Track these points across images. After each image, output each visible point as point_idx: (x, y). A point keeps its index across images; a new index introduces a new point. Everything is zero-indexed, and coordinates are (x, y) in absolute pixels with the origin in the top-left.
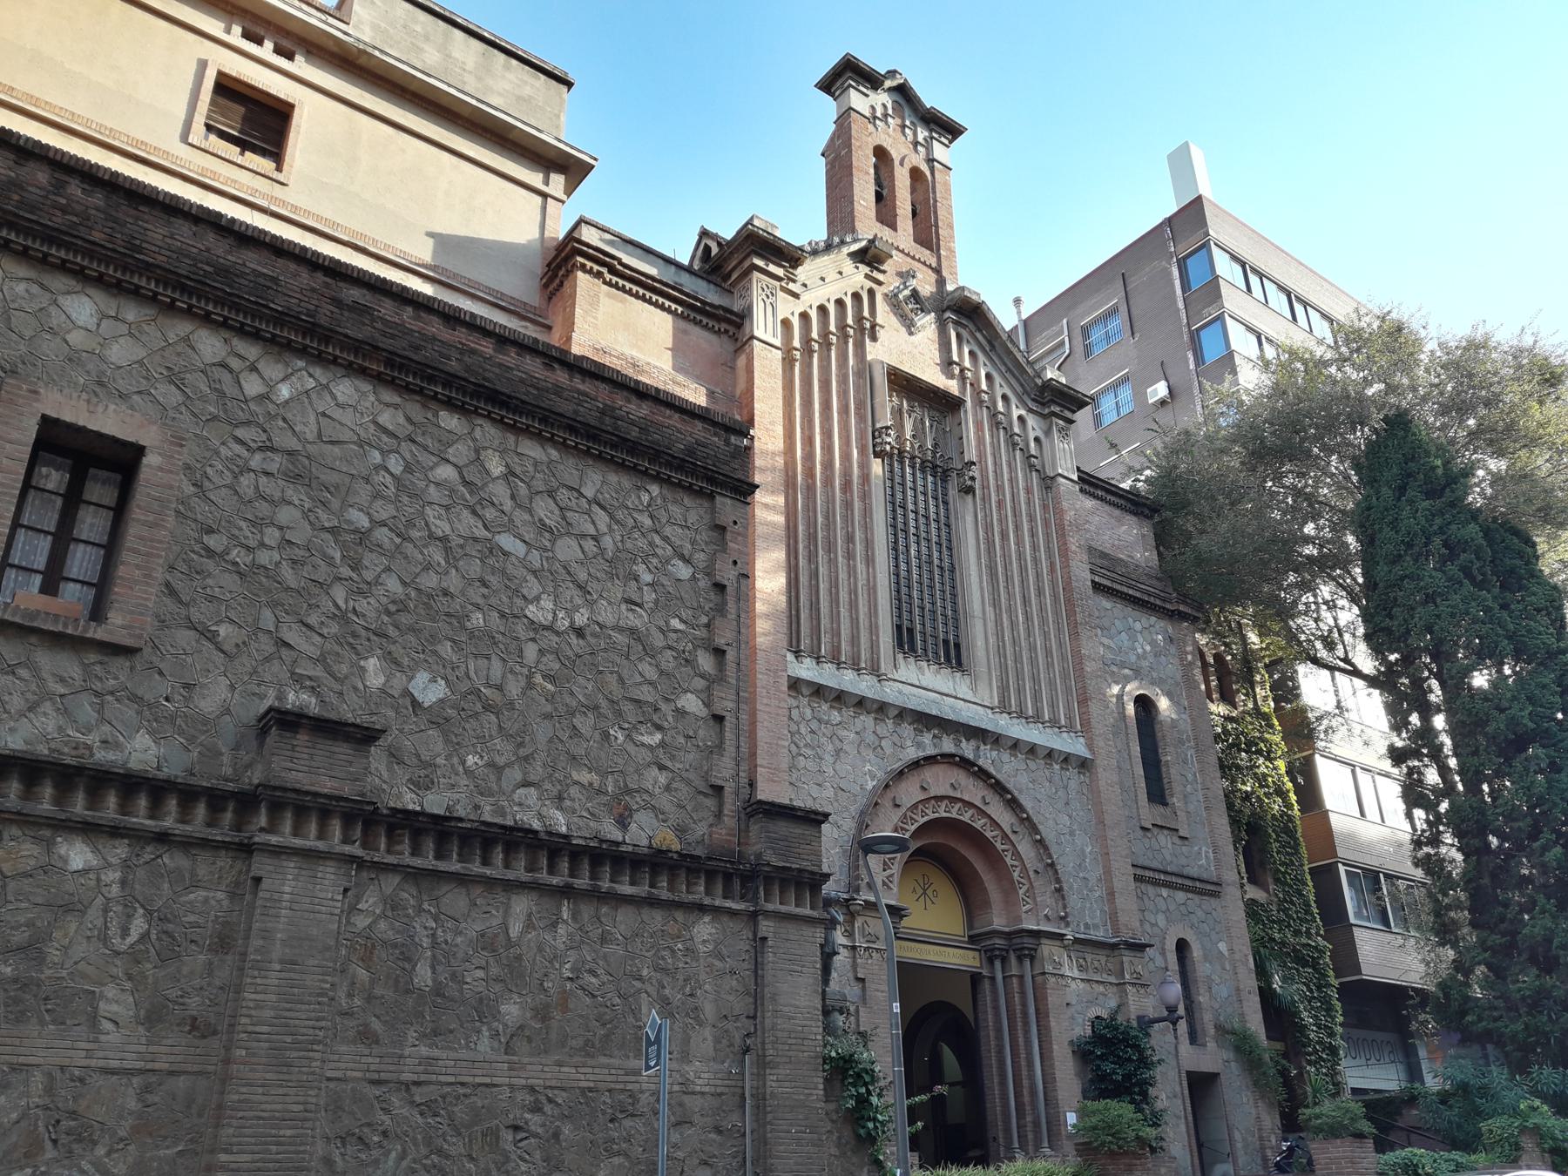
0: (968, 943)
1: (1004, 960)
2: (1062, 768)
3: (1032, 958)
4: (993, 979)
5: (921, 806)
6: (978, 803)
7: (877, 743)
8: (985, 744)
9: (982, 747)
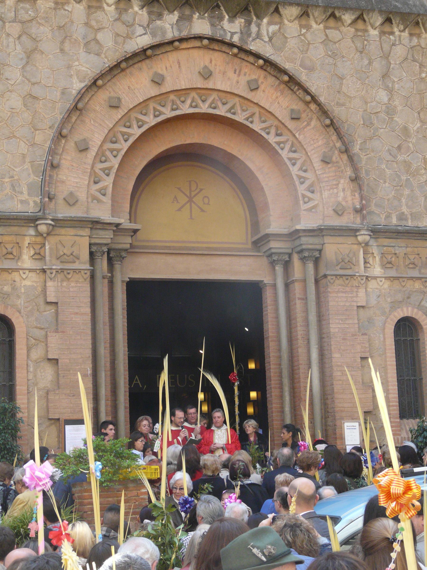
2: (382, 33)
3: (317, 261)
4: (274, 286)
5: (152, 105)
6: (242, 91)
7: (93, 36)
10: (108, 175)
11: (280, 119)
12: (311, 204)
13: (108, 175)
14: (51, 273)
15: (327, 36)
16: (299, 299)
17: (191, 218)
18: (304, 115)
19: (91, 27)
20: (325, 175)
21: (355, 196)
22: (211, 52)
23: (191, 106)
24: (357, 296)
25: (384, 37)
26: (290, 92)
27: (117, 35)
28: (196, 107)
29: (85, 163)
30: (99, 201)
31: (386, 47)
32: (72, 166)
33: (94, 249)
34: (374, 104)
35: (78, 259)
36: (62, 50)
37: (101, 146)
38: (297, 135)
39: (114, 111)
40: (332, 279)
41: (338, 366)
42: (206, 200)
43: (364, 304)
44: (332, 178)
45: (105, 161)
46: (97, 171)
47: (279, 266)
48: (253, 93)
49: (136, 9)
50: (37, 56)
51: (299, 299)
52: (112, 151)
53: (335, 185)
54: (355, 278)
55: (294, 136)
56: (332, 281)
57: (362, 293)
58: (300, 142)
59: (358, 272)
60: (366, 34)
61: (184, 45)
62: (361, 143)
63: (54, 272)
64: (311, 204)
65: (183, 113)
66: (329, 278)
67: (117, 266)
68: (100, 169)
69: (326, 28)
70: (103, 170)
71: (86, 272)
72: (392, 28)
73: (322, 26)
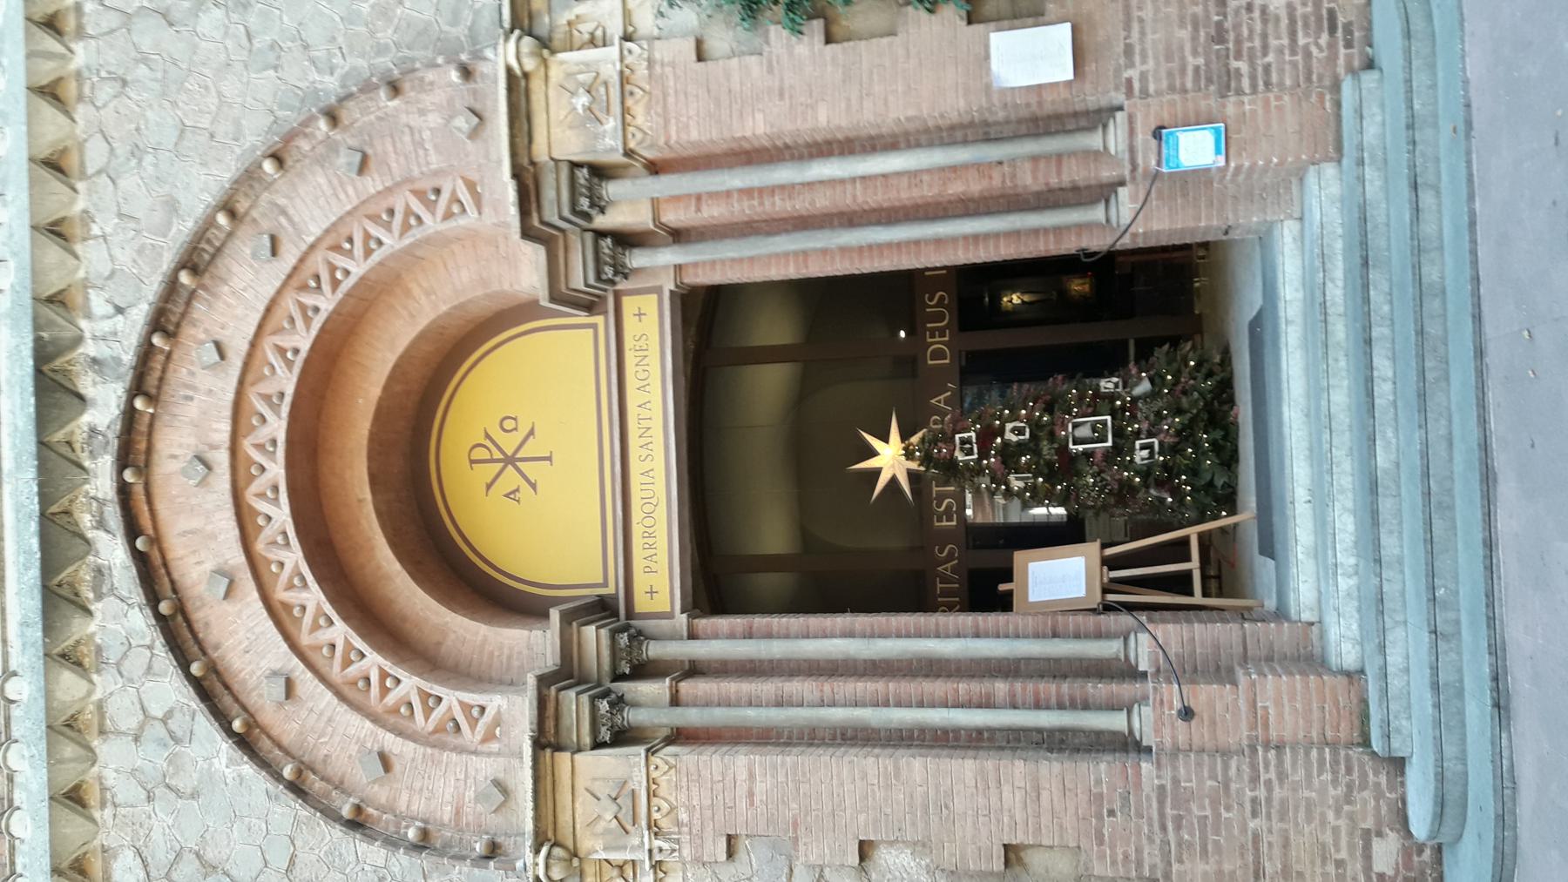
0: (605, 313)
1: (626, 240)
2: (80, 33)
3: (600, 172)
7: (159, 726)
8: (78, 340)
9: (90, 349)
10: (439, 699)
11: (278, 284)
12: (464, 196)
13: (439, 699)
14: (661, 850)
15: (99, 172)
16: (698, 210)
17: (549, 459)
18: (265, 224)
19: (141, 727)
20: (394, 165)
21: (432, 83)
22: (155, 458)
23: (276, 501)
24: (673, 64)
25: (90, 31)
26: (219, 262)
27: (150, 668)
28: (275, 489)
29: (413, 760)
30: (497, 721)
31: (113, 20)
32: (421, 790)
33: (605, 735)
34: (229, 43)
35: (625, 782)
36: (194, 795)
37: (375, 719)
38: (311, 239)
39: (300, 690)
40: (633, 135)
41: (849, 106)
42: (509, 424)
43: (690, 46)
44: (399, 145)
45: (410, 705)
46: (431, 726)
47: (627, 261)
48: (230, 354)
49: (92, 627)
50: (210, 855)
51: (698, 210)
52: (385, 691)
53: (412, 134)
54: (627, 72)
55: (312, 247)
56: (639, 136)
57: (662, 51)
58: (327, 231)
59: (614, 65)
60: (86, 74)
61: (145, 521)
62: (319, 71)
63: (657, 843)
64: (464, 196)
65: (290, 520)
66: (632, 145)
67: (654, 650)
68: (427, 719)
69: (83, 175)
70: (428, 712)
71: (652, 768)
72: (67, 9)
73: (80, 186)
